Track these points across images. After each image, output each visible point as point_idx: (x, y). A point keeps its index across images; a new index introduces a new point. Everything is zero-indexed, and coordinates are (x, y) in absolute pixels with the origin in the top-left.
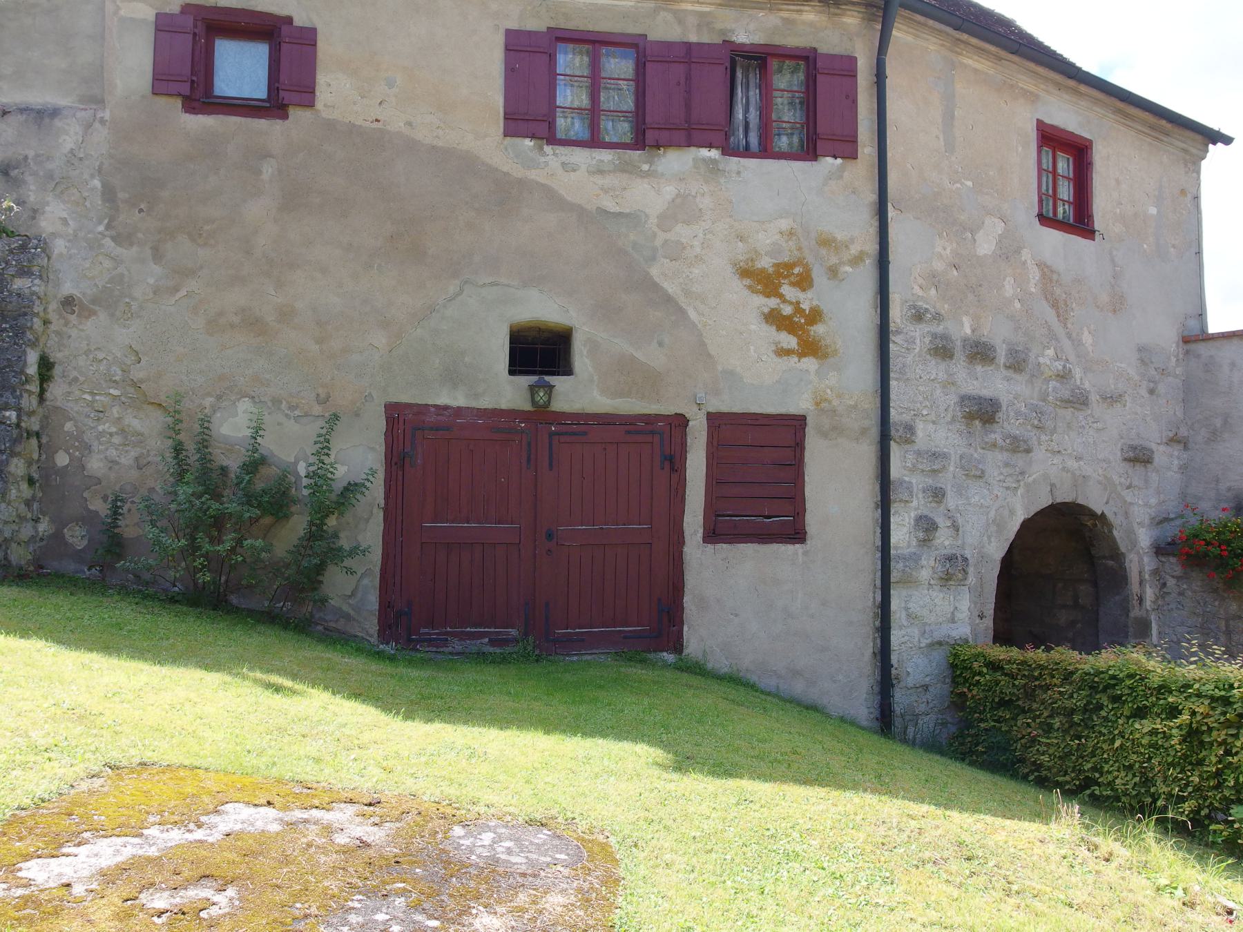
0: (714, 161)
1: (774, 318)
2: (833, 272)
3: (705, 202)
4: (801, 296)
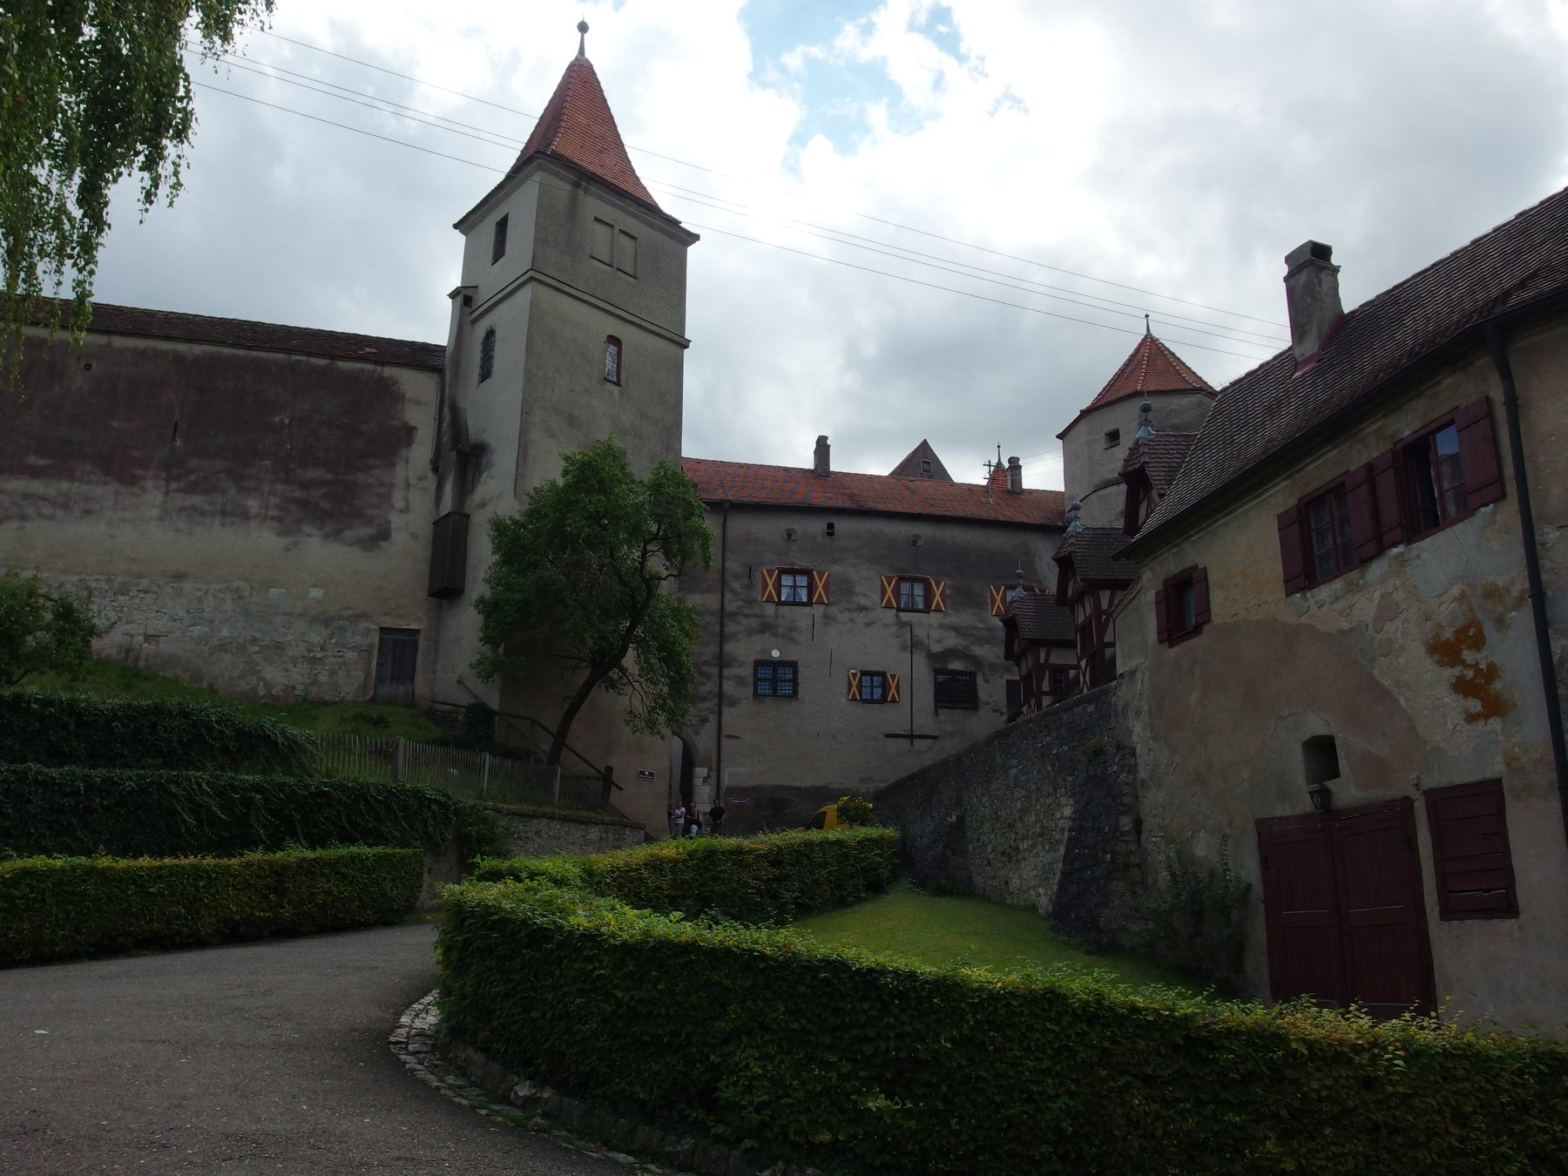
0: (1401, 554)
1: (1462, 687)
2: (1501, 623)
3: (1398, 596)
4: (1478, 656)
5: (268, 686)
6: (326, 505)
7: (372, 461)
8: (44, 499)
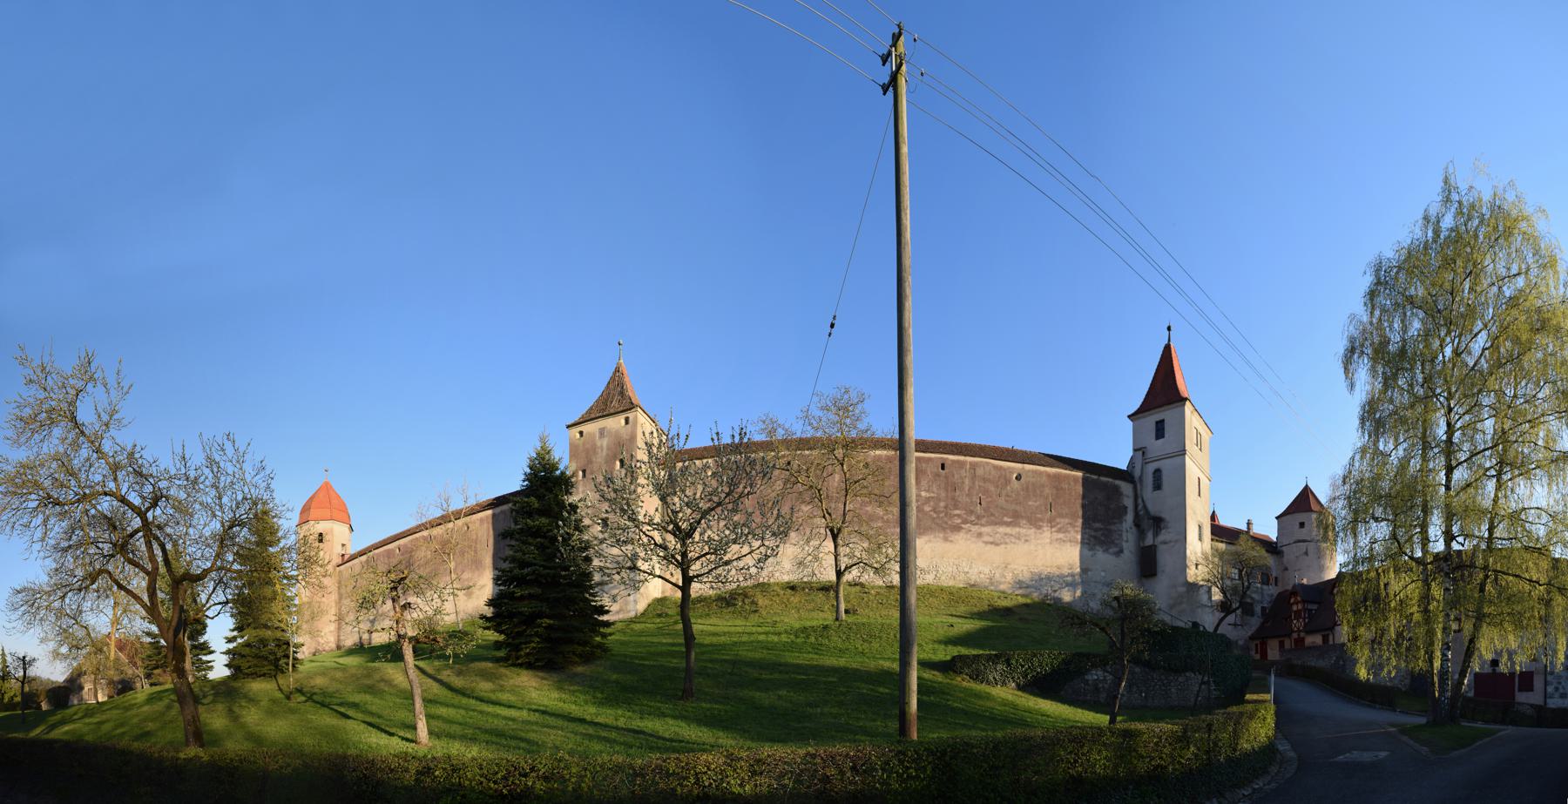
5: (1092, 609)
6: (1103, 538)
7: (1116, 521)
8: (1012, 535)
